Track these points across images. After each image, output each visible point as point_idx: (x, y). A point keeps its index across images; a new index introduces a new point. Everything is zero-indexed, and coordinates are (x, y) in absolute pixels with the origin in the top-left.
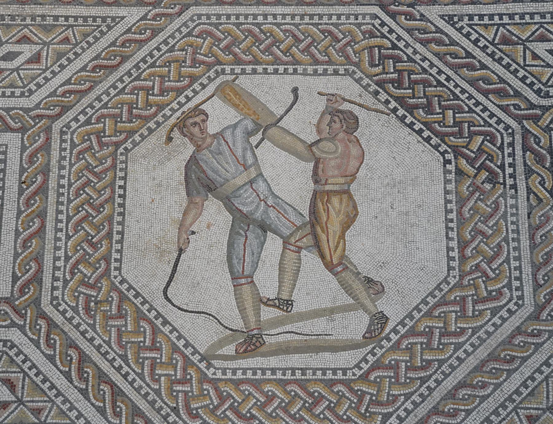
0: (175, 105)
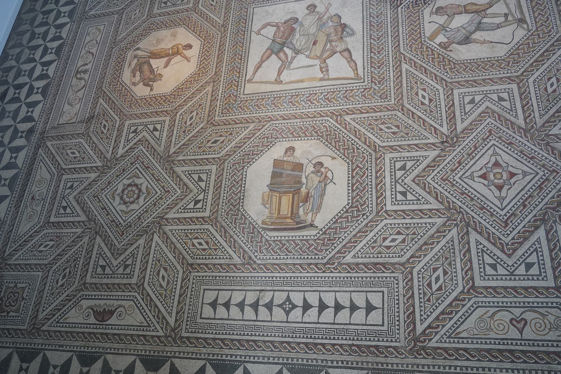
0: (438, 51)
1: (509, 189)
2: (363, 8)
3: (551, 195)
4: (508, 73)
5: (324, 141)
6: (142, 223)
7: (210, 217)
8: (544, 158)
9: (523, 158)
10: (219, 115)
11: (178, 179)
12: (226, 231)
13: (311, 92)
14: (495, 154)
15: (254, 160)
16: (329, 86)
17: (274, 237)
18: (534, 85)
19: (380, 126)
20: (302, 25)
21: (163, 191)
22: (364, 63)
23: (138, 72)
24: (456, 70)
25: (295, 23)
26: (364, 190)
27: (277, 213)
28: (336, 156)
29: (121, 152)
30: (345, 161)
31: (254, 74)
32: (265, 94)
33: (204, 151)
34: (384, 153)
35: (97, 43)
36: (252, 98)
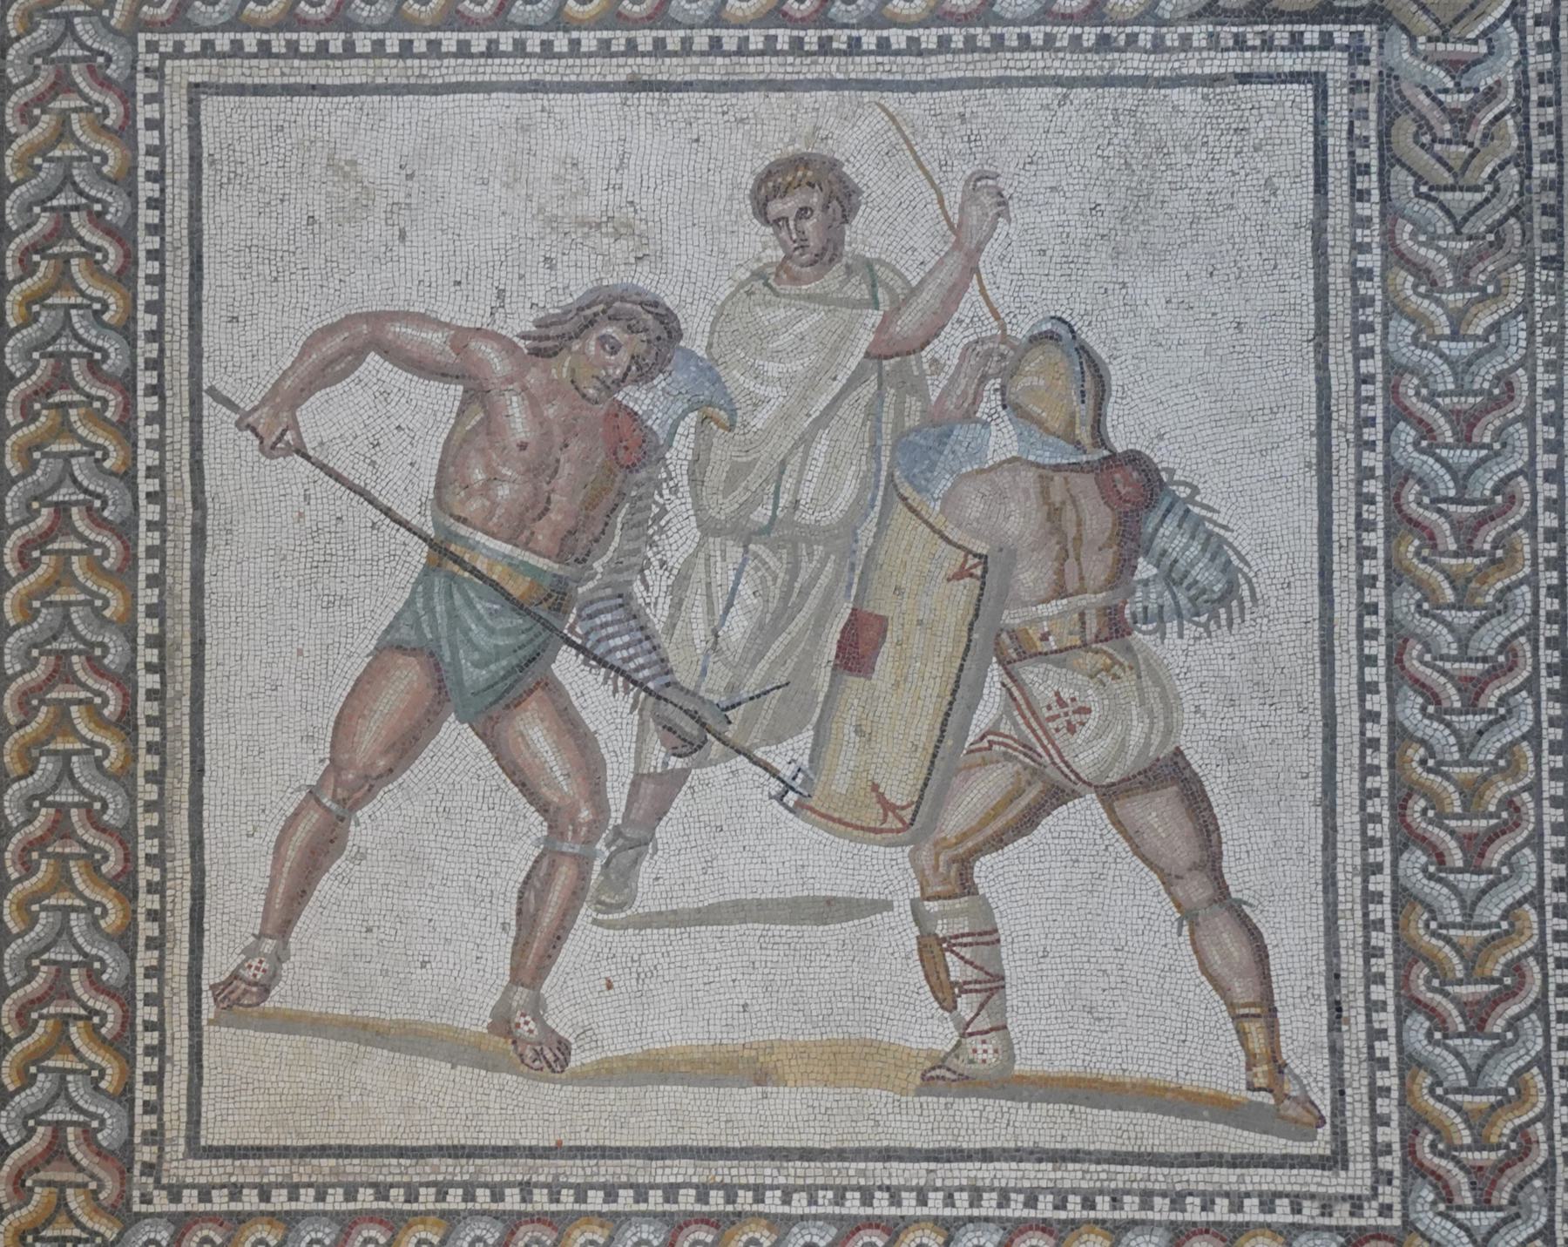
20: (716, 409)
25: (642, 372)
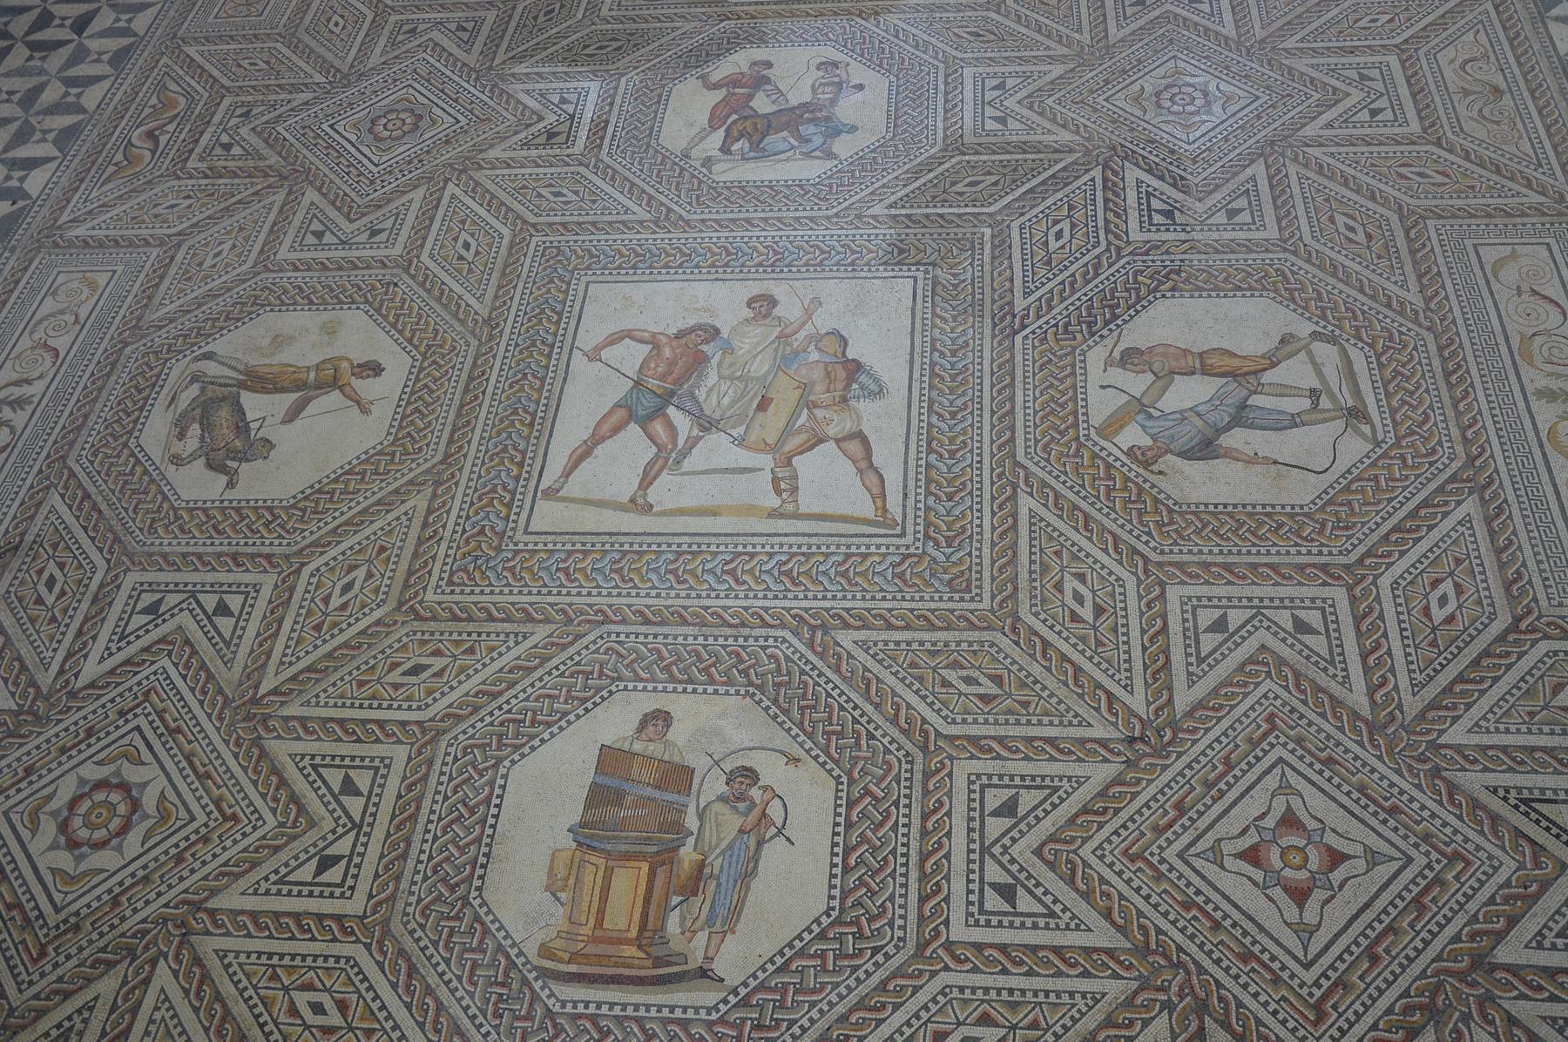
0: (1125, 470)
1: (1327, 901)
2: (913, 323)
3: (1450, 931)
4: (1320, 553)
5: (766, 703)
6: (123, 919)
7: (365, 916)
8: (1426, 814)
9: (1365, 807)
10: (438, 586)
11: (274, 779)
12: (412, 971)
13: (740, 549)
14: (1285, 788)
15: (536, 742)
16: (797, 535)
17: (575, 1004)
18: (1395, 597)
19: (944, 672)
20: (728, 349)
21: (216, 814)
22: (905, 479)
23: (196, 426)
24: (1176, 531)
26: (881, 869)
27: (592, 922)
28: (801, 753)
29: (91, 669)
30: (830, 772)
31: (567, 474)
32: (595, 539)
33: (374, 697)
34: (951, 758)
35: (76, 321)
36: (550, 546)
